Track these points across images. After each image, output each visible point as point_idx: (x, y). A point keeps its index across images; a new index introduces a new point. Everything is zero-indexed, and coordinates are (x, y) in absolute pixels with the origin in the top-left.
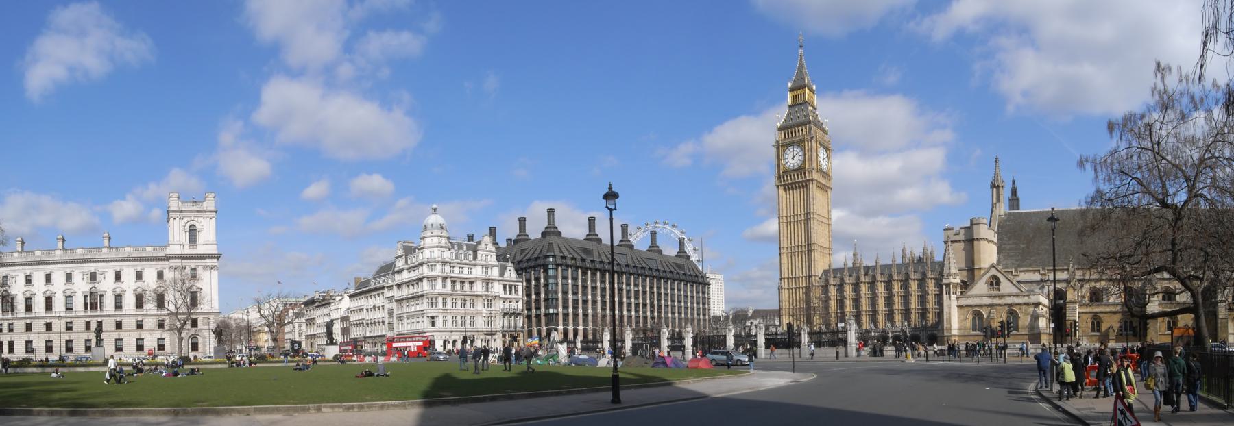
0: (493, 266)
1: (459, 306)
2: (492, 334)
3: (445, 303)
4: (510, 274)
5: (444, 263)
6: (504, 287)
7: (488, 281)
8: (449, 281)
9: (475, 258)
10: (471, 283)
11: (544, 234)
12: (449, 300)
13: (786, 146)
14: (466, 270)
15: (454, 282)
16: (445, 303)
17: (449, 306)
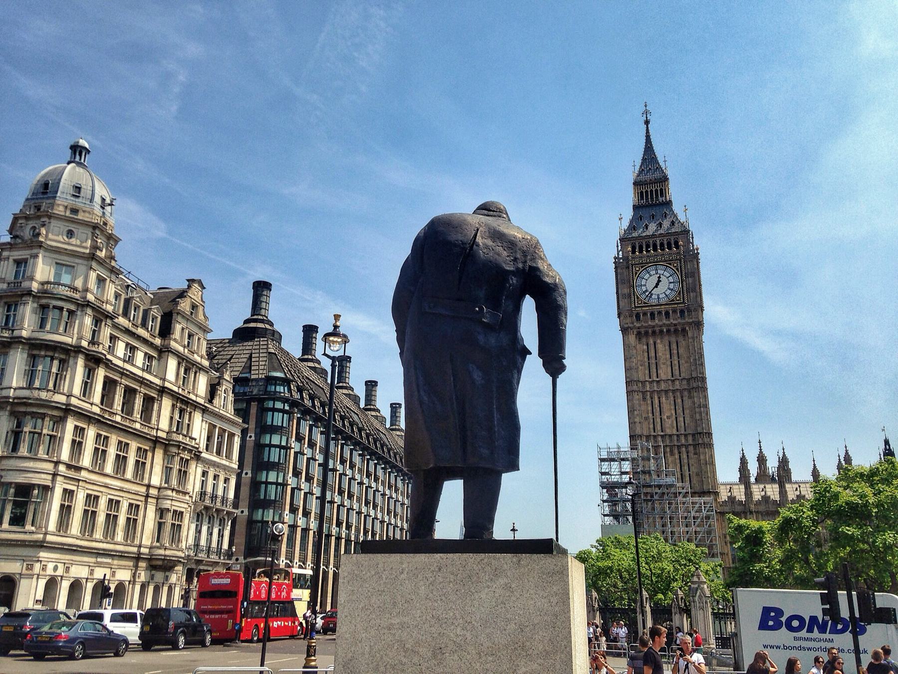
0: (201, 368)
1: (109, 468)
2: (167, 566)
3: (77, 446)
4: (225, 403)
5: (101, 317)
6: (212, 427)
7: (184, 404)
8: (101, 374)
9: (165, 331)
10: (149, 401)
11: (243, 334)
12: (91, 432)
13: (644, 266)
14: (140, 358)
15: (109, 385)
16: (77, 446)
17: (86, 460)
